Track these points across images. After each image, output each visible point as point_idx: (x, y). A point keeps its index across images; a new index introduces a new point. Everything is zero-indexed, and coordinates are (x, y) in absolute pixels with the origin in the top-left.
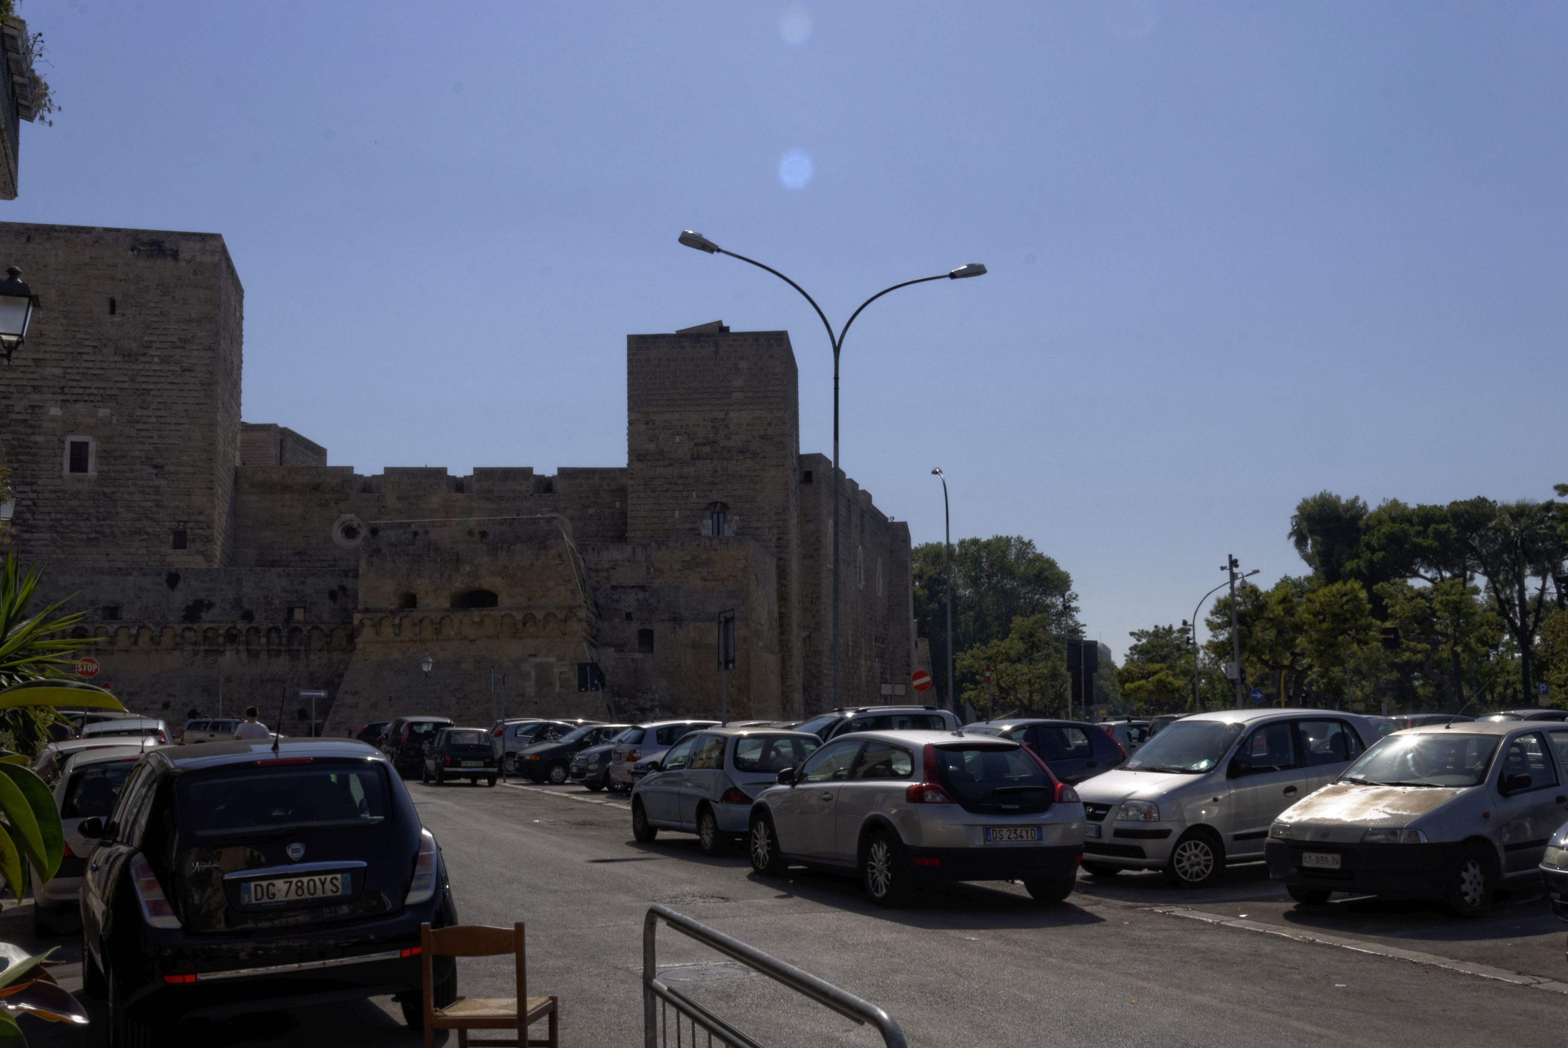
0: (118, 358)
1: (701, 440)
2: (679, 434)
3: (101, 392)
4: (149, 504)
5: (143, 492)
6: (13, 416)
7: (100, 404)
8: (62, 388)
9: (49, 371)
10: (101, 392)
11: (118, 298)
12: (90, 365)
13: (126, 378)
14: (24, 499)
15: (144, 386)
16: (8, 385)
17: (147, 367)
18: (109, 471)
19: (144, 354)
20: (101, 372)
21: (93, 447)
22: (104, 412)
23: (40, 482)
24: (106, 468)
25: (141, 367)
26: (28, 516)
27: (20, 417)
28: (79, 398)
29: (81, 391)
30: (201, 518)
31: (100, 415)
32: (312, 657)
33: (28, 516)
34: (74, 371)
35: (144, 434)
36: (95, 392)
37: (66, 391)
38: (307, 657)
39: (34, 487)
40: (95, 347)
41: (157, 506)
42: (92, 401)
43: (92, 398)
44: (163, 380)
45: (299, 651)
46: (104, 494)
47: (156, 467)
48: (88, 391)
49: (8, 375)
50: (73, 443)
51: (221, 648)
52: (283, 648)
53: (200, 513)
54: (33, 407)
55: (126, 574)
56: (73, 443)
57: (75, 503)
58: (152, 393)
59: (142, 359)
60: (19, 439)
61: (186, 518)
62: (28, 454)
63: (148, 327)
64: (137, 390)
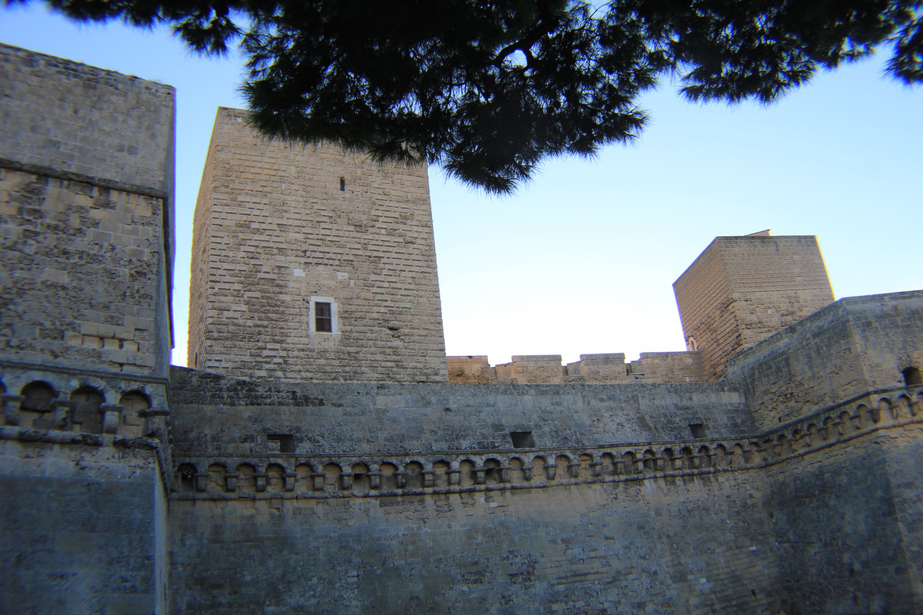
0: (352, 228)
1: (785, 312)
2: (769, 308)
3: (339, 257)
4: (390, 364)
5: (384, 353)
6: (260, 275)
7: (338, 268)
8: (305, 252)
9: (292, 236)
10: (339, 257)
11: (348, 178)
12: (328, 232)
13: (359, 246)
14: (275, 357)
15: (376, 254)
16: (257, 247)
17: (377, 237)
18: (351, 331)
19: (373, 226)
20: (338, 239)
21: (335, 308)
22: (342, 276)
23: (289, 340)
24: (348, 328)
25: (371, 237)
26: (279, 374)
27: (268, 276)
28: (320, 261)
29: (321, 255)
30: (437, 378)
31: (339, 278)
32: (721, 479)
33: (279, 374)
34: (315, 237)
35: (379, 297)
36: (334, 256)
37: (308, 254)
38: (717, 480)
39: (283, 345)
40: (331, 217)
41: (397, 366)
42: (331, 265)
43: (331, 262)
44: (390, 249)
45: (709, 473)
46: (349, 353)
47: (391, 329)
48: (328, 256)
49: (256, 237)
50: (317, 304)
51: (641, 476)
52: (696, 471)
53: (436, 374)
54: (279, 267)
55: (523, 393)
56: (317, 304)
57: (322, 361)
58: (383, 260)
59: (371, 230)
60: (268, 297)
61: (424, 378)
62: (276, 312)
63: (374, 204)
64: (370, 257)
